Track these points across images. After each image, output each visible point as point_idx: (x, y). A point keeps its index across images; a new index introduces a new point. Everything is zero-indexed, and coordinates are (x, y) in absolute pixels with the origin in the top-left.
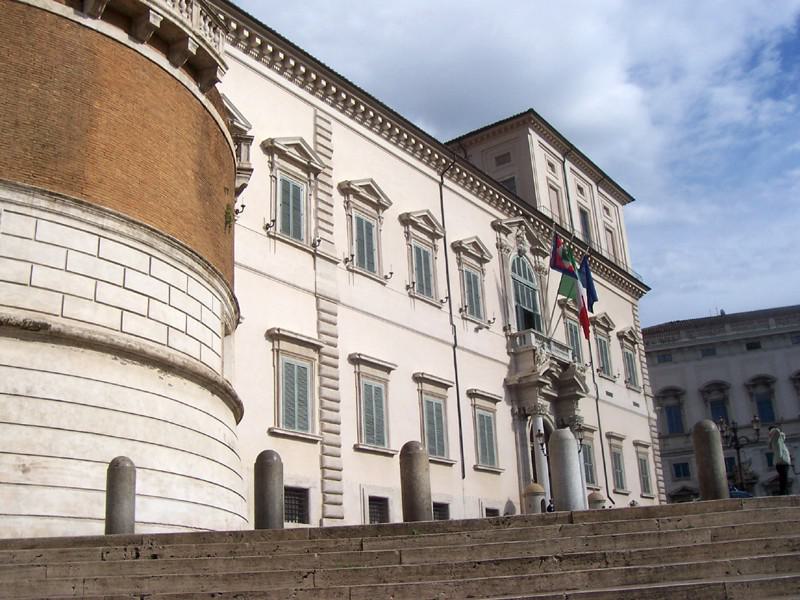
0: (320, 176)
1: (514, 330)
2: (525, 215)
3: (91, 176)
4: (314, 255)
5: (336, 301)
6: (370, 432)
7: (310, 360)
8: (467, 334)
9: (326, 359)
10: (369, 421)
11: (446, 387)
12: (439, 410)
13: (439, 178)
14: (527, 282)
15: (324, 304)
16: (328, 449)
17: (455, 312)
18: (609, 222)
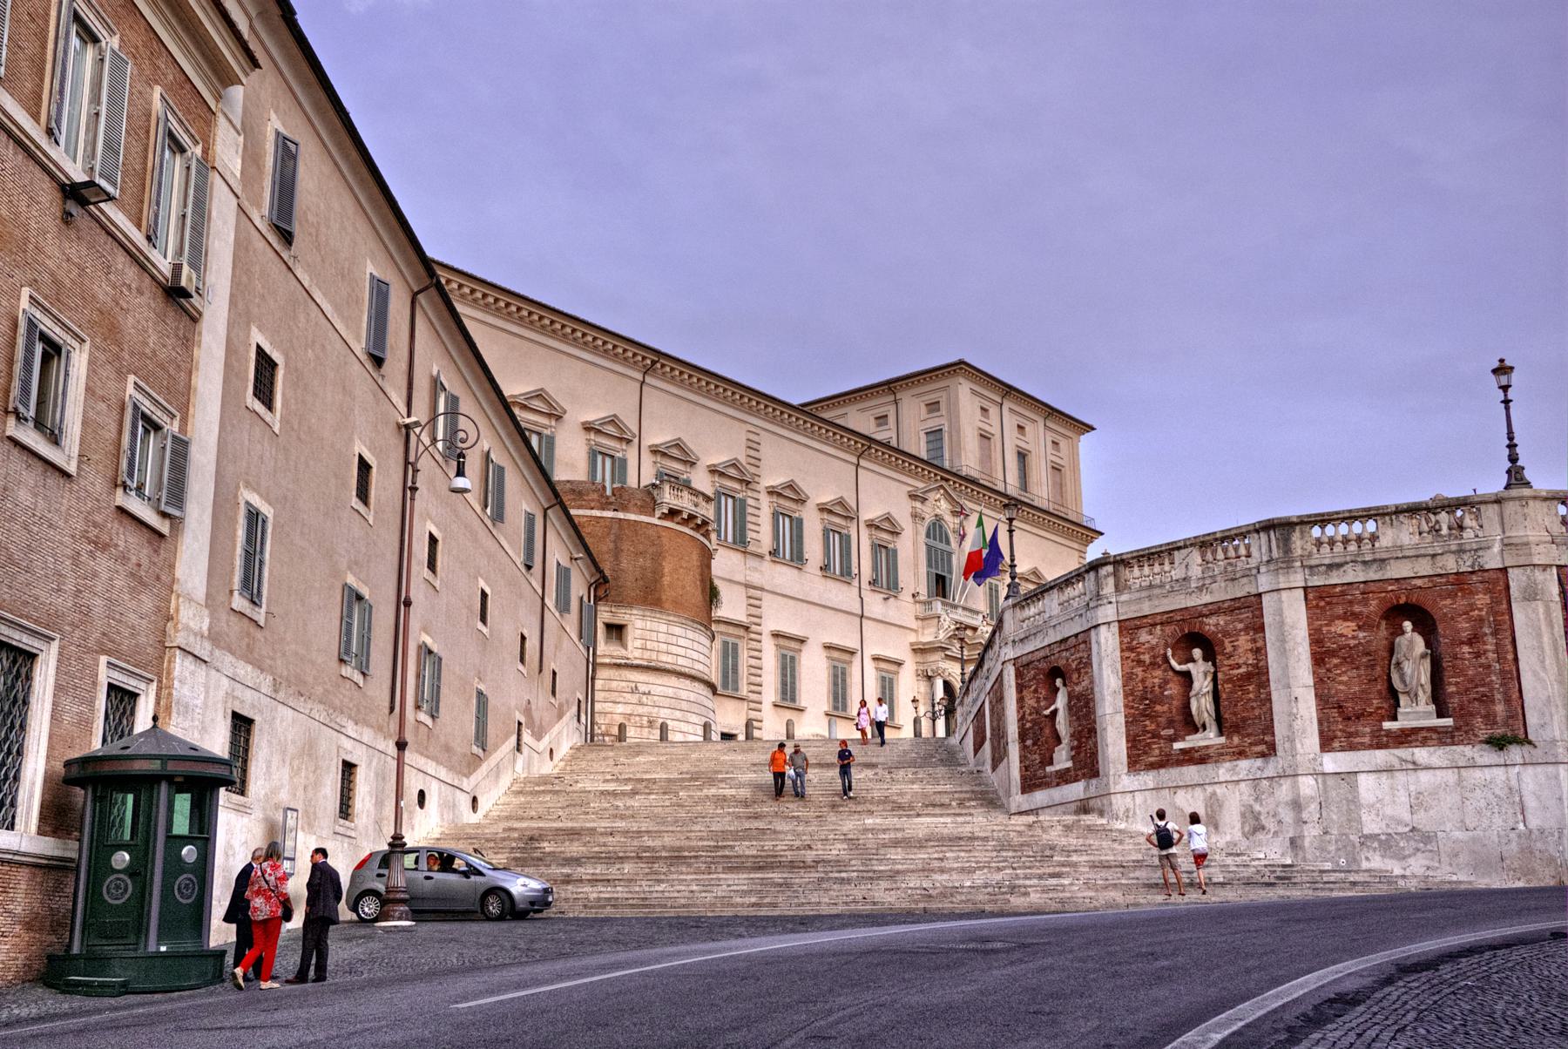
0: (750, 486)
1: (923, 597)
2: (942, 478)
3: (664, 597)
4: (744, 552)
5: (762, 589)
6: (784, 692)
7: (739, 637)
8: (875, 604)
9: (753, 636)
10: (784, 684)
11: (852, 653)
12: (844, 674)
13: (854, 460)
14: (942, 546)
15: (752, 592)
16: (753, 705)
17: (865, 585)
18: (1058, 461)
